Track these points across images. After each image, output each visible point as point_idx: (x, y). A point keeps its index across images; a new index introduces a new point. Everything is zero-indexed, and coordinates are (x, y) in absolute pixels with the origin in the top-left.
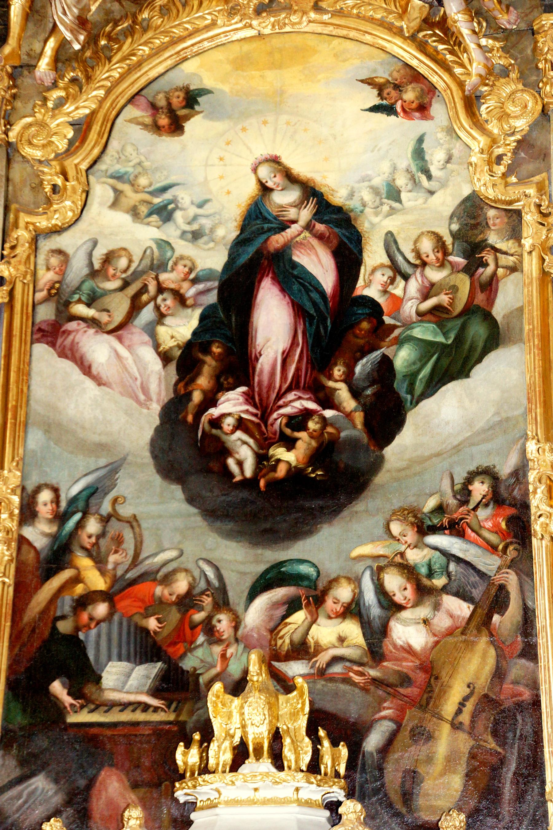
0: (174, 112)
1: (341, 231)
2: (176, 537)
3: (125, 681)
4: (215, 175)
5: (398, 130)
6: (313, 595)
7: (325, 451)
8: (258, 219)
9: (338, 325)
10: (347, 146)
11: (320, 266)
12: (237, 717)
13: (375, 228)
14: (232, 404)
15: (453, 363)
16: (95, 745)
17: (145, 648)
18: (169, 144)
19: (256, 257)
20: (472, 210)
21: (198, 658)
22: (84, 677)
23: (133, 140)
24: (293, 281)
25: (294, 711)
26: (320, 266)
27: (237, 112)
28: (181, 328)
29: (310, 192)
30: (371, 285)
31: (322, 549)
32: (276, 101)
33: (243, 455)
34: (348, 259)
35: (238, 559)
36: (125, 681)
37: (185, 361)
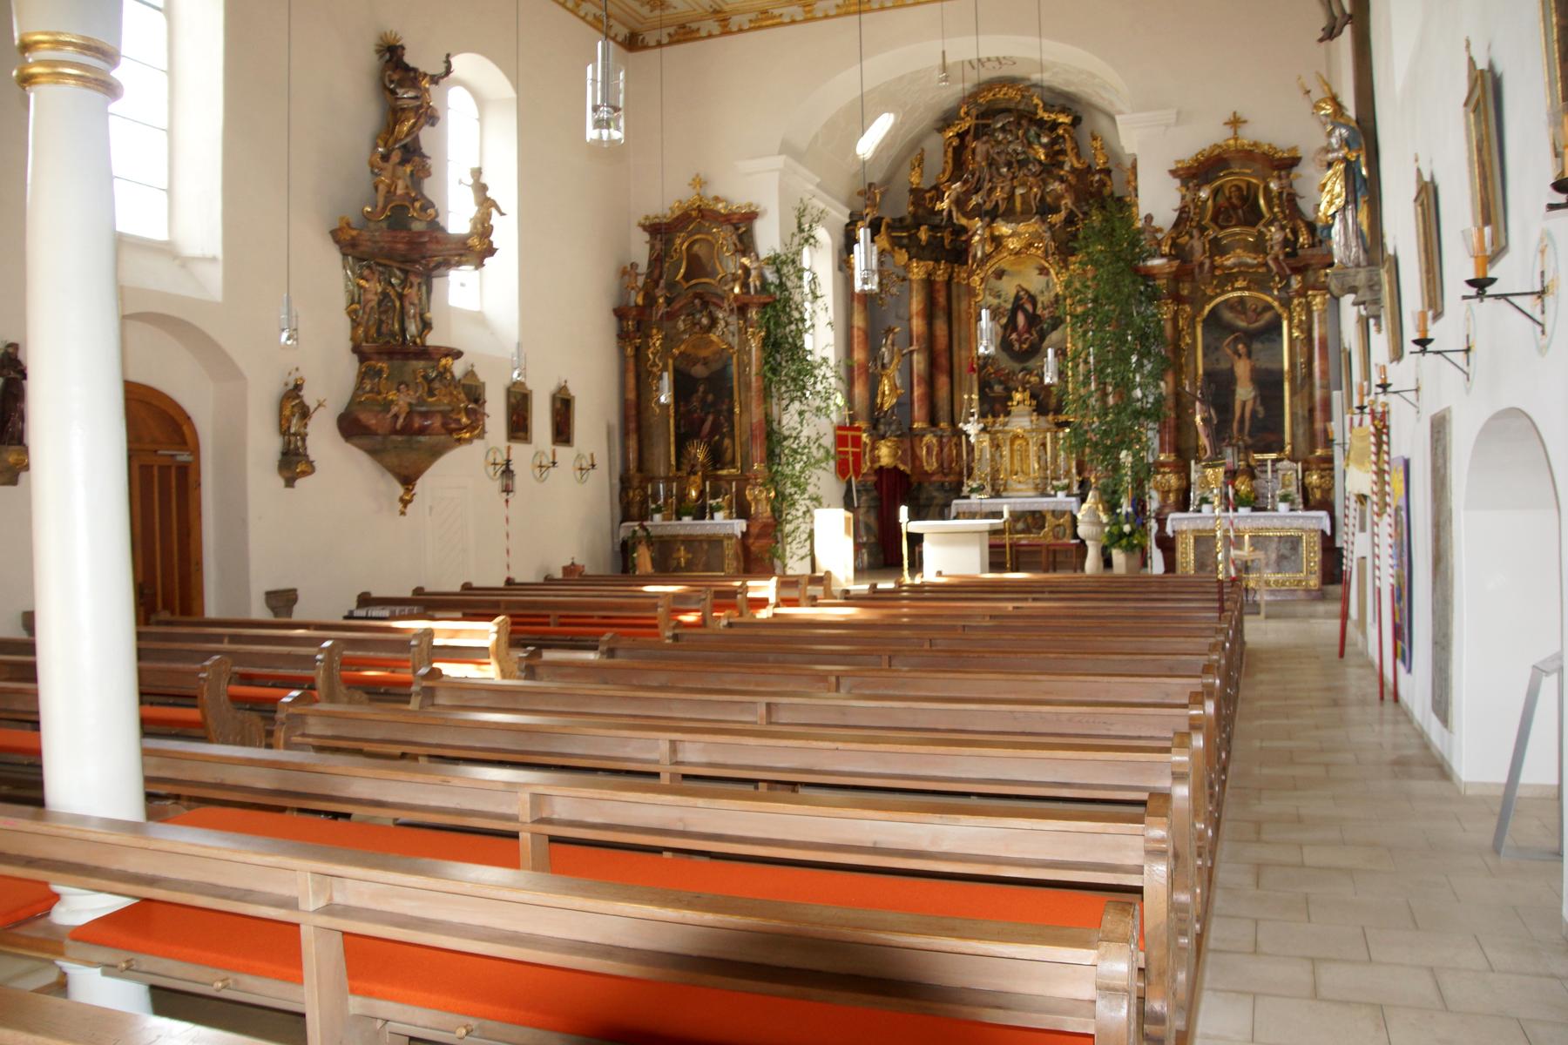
0: (1000, 274)
1: (1033, 299)
2: (1006, 363)
3: (998, 388)
4: (1009, 287)
5: (1043, 279)
6: (1030, 372)
7: (1032, 345)
8: (1017, 298)
9: (1033, 319)
10: (1034, 282)
11: (1029, 307)
12: (1018, 396)
13: (1040, 299)
14: (1014, 336)
15: (1054, 327)
16: (994, 399)
17: (1001, 383)
18: (998, 283)
19: (1017, 306)
20: (1057, 295)
21: (1011, 384)
22: (991, 388)
23: (993, 282)
24: (1025, 311)
25: (1027, 394)
26: (1029, 307)
27: (1012, 275)
28: (1004, 321)
29: (1027, 292)
30: (1039, 312)
31: (1031, 364)
32: (1019, 272)
33: (1017, 346)
34: (1035, 305)
35: (1017, 366)
36: (998, 388)
37: (1005, 327)
